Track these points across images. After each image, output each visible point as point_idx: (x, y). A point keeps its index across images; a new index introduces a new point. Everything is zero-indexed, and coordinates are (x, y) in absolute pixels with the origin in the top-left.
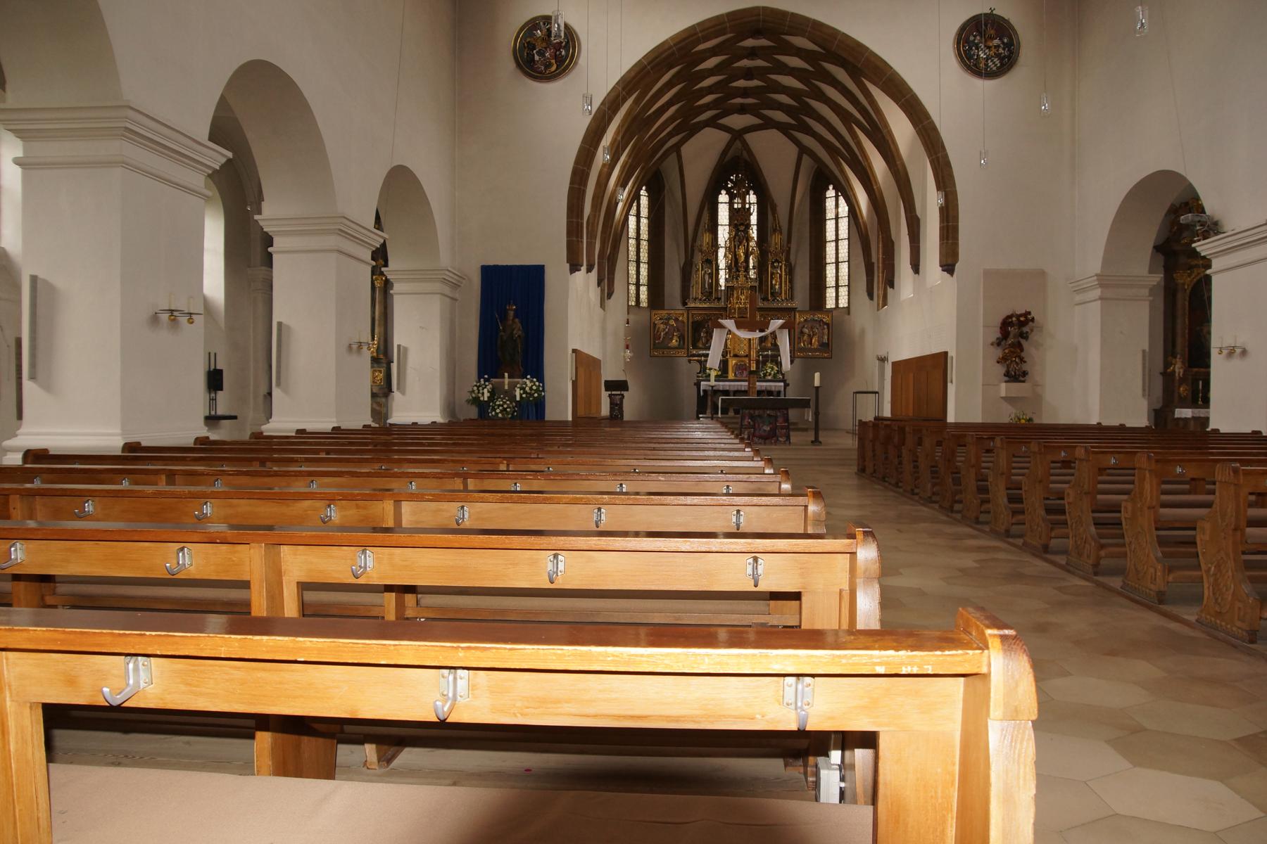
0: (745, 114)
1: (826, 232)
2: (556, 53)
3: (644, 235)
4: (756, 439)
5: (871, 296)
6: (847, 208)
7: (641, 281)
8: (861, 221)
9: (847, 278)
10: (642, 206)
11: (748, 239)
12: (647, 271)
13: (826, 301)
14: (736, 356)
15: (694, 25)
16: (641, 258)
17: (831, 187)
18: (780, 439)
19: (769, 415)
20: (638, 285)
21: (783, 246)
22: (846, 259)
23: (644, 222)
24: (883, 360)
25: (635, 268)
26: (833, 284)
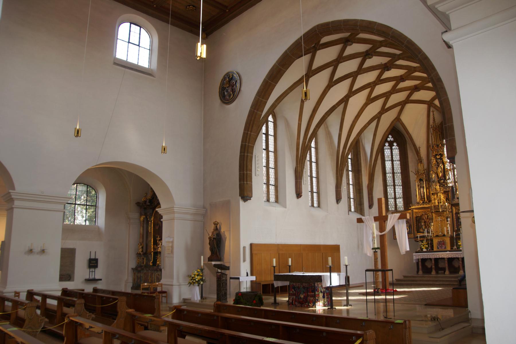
0: (419, 91)
2: (232, 88)
4: (296, 303)
7: (397, 196)
12: (401, 190)
14: (437, 236)
15: (286, 52)
16: (397, 183)
18: (310, 305)
19: (304, 287)
20: (395, 198)
25: (393, 189)
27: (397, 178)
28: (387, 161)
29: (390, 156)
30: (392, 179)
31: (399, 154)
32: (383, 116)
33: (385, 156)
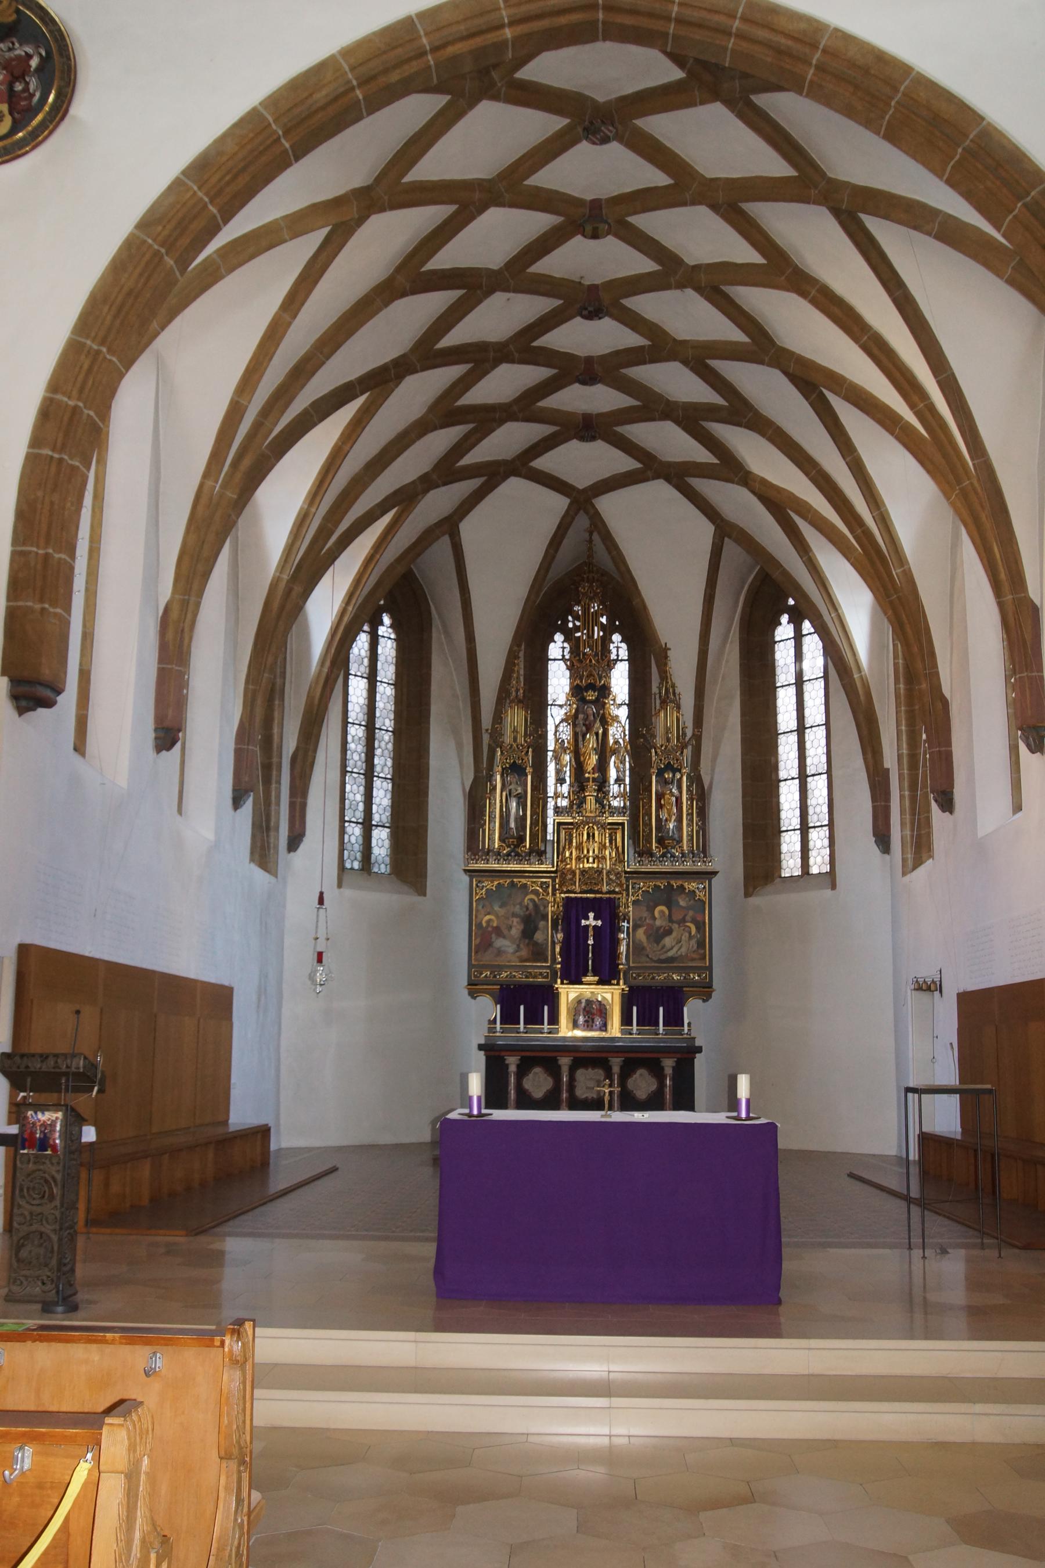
0: (593, 439)
1: (775, 715)
3: (385, 719)
5: (883, 840)
6: (820, 661)
7: (376, 819)
8: (856, 676)
9: (825, 809)
10: (381, 658)
11: (605, 721)
12: (389, 796)
13: (780, 862)
16: (378, 769)
17: (784, 619)
20: (367, 825)
21: (684, 734)
22: (823, 768)
23: (386, 693)
24: (929, 987)
25: (362, 789)
26: (796, 822)
27: (379, 747)
28: (356, 675)
29: (366, 661)
30: (365, 748)
31: (394, 662)
32: (432, 494)
33: (351, 656)
